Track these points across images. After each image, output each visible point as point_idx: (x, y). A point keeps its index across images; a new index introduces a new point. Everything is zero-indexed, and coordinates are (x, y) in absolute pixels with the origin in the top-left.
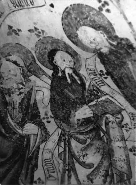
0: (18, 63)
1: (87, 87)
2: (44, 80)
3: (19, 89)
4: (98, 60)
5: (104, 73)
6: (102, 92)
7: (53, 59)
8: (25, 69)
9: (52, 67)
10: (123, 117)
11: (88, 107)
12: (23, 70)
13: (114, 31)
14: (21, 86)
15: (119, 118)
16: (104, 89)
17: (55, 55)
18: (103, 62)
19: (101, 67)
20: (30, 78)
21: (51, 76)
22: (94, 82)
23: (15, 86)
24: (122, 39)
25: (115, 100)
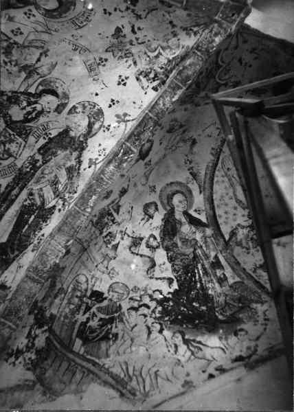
0: (39, 63)
1: (27, 124)
2: (23, 86)
3: (10, 62)
4: (61, 130)
5: (50, 136)
6: (27, 136)
7: (48, 93)
8: (32, 68)
9: (38, 92)
10: (7, 159)
11: (4, 127)
12: (30, 66)
13: (91, 137)
14: (13, 63)
15: (3, 155)
16: (32, 139)
17: (52, 95)
18: (60, 134)
19: (54, 133)
20: (23, 73)
21: (29, 91)
22: (36, 130)
23: (14, 58)
24: (86, 143)
25: (23, 150)
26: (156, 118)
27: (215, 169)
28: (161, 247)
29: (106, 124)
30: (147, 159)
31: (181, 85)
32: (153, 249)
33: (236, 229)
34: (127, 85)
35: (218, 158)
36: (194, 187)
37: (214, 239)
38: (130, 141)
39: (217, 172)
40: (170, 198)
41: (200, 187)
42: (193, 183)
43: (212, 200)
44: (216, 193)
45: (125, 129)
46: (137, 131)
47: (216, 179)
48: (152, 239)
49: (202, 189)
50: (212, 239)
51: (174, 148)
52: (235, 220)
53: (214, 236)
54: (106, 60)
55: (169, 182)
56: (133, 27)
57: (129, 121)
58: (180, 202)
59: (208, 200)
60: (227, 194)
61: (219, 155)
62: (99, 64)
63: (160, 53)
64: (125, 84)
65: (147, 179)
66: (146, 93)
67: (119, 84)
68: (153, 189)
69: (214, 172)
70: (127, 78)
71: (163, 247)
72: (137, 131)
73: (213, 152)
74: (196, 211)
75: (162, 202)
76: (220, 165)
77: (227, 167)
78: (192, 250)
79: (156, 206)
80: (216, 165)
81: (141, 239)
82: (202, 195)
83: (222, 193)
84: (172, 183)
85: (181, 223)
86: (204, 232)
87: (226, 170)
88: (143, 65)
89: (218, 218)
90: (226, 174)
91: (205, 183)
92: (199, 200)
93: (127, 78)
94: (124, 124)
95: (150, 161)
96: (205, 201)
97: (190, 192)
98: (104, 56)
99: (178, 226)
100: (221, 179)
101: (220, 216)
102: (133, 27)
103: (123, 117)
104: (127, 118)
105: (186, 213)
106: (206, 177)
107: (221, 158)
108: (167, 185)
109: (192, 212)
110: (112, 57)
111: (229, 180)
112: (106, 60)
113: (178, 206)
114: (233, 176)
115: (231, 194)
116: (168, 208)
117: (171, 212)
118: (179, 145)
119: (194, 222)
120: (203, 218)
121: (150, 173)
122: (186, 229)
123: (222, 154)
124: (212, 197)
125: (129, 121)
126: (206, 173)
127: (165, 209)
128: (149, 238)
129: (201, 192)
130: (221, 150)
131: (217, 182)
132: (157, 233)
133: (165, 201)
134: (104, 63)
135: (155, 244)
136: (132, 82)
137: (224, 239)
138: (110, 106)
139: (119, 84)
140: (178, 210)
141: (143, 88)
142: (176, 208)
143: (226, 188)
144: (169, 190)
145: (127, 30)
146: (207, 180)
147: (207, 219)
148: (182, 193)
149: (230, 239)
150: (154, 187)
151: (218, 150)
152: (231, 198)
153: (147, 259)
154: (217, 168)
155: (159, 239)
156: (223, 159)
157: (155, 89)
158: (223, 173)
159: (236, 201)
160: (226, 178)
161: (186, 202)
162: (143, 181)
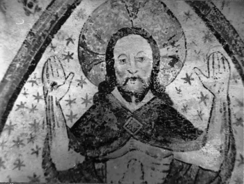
27: (26, 77)
39: (27, 85)
44: (11, 128)
47: (20, 99)
61: (42, 51)
69: (22, 83)
76: (38, 72)
77: (52, 79)
83: (22, 135)
87: (48, 86)
90: (46, 95)
111: (47, 109)
114: (57, 104)
115: (40, 143)
123: (48, 49)
130: (48, 42)
131: (22, 106)
143: (34, 125)
151: (43, 40)
154: (31, 77)
158: (41, 94)
159: (44, 163)
160: (42, 102)
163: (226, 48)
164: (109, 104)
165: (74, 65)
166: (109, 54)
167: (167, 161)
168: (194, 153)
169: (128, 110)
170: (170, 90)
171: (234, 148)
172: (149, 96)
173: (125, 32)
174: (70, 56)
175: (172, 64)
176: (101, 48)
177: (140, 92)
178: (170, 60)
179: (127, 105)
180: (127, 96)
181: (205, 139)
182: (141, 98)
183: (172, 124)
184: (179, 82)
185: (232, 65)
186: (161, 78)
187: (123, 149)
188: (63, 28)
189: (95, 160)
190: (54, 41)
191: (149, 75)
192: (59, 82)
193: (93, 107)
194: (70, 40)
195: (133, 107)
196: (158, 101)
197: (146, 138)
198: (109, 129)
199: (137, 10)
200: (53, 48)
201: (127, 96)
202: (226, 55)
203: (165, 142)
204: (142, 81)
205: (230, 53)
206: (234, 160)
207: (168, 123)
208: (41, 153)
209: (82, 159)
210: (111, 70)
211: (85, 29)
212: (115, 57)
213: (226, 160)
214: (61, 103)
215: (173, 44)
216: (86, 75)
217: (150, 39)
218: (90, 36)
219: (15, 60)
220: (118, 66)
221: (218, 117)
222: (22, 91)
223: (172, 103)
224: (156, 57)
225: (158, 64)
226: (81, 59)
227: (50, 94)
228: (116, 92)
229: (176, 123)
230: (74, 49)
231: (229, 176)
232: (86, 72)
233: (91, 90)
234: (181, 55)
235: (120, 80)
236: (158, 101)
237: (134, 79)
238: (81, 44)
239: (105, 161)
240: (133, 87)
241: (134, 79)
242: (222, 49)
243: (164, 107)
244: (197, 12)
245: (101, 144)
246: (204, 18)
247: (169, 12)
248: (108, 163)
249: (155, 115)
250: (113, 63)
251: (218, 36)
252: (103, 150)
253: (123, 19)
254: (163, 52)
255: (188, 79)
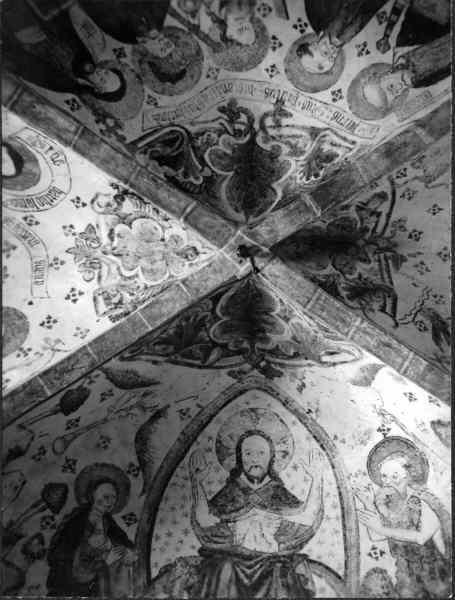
26: (95, 357)
27: (178, 464)
28: (45, 559)
29: (26, 346)
30: (73, 416)
31: (147, 323)
32: (31, 557)
33: (175, 564)
34: (78, 302)
35: (186, 451)
36: (137, 485)
37: (134, 571)
38: (45, 377)
39: (178, 469)
40: (93, 485)
41: (145, 484)
42: (136, 476)
43: (157, 509)
44: (167, 499)
45: (49, 361)
46: (62, 366)
48: (36, 541)
49: (147, 489)
50: (131, 569)
51: (124, 413)
52: (178, 550)
53: (136, 564)
54: (62, 263)
55: (100, 462)
56: (112, 231)
57: (59, 350)
58: (106, 497)
59: (150, 508)
60: (182, 507)
62: (51, 265)
63: (137, 276)
64: (75, 301)
65: (66, 447)
66: (98, 321)
67: (68, 298)
68: (70, 465)
69: (175, 469)
70: (81, 293)
71: (48, 559)
72: (62, 366)
73: (182, 437)
74: (124, 517)
75: (77, 489)
76: (186, 460)
78: (91, 577)
79: (66, 491)
80: (182, 458)
81: (20, 537)
82: (144, 497)
84: (104, 465)
85: (93, 530)
86: (123, 554)
87: (194, 470)
88: (110, 282)
89: (153, 540)
91: (155, 479)
92: (136, 503)
93: (81, 293)
94: (51, 352)
95: (77, 420)
96: (144, 507)
97: (128, 487)
98: (63, 256)
99: (87, 533)
100: (180, 481)
101: (158, 538)
102: (112, 231)
103: (53, 344)
104: (58, 347)
105: (107, 517)
106: (159, 471)
107: (191, 451)
108: (96, 465)
109: (117, 518)
110: (72, 261)
112: (62, 263)
113: (100, 502)
114: (201, 485)
115: (188, 508)
116: (84, 501)
117: (84, 510)
118: (132, 411)
119: (115, 535)
120: (131, 537)
121: (75, 437)
122: (97, 540)
123: (195, 444)
124: (158, 504)
125: (59, 350)
126: (162, 467)
127: (78, 499)
128: (33, 538)
129: (144, 491)
130: (195, 439)
131: (174, 484)
132: (48, 535)
133: (83, 489)
134: (59, 265)
135: (35, 548)
136: (85, 302)
137: (149, 573)
138: (42, 324)
139: (68, 298)
140: (97, 509)
141: (97, 312)
142: (95, 505)
144: (97, 473)
145: (103, 233)
146: (159, 479)
147: (136, 535)
148: (114, 484)
149: (158, 577)
150: (75, 462)
152: (186, 516)
153: (15, 572)
154: (181, 465)
155: (47, 545)
156: (193, 453)
157: (113, 319)
159: (192, 522)
161: (114, 500)
162: (59, 446)
163: (322, 446)
164: (238, 485)
165: (212, 457)
166: (239, 449)
167: (278, 521)
168: (298, 516)
169: (251, 489)
170: (282, 475)
171: (323, 511)
172: (267, 479)
173: (250, 433)
174: (210, 450)
175: (284, 457)
176: (233, 445)
177: (260, 476)
178: (283, 454)
179: (251, 485)
180: (251, 479)
181: (305, 508)
182: (261, 480)
183: (283, 499)
184: (289, 469)
185: (326, 457)
186: (275, 467)
187: (248, 515)
188: (207, 429)
189: (228, 521)
190: (199, 439)
191: (267, 464)
192: (202, 468)
193: (226, 487)
194: (210, 438)
195: (255, 486)
196: (274, 483)
197: (264, 507)
198: (238, 502)
199: (259, 419)
200: (198, 443)
201: (251, 479)
202: (321, 450)
203: (277, 509)
204: (261, 468)
205: (324, 449)
206: (322, 518)
207: (280, 499)
208: (189, 516)
209: (218, 521)
210: (239, 460)
211: (221, 430)
212: (243, 450)
213: (317, 519)
214: (204, 483)
215: (284, 442)
216: (222, 464)
217: (268, 439)
218: (225, 436)
219: (171, 451)
220: (245, 458)
221: (315, 492)
222: (175, 474)
223: (283, 484)
224: (273, 452)
225: (274, 456)
226: (218, 452)
227: (195, 476)
228: (243, 476)
229: (286, 497)
230: (212, 444)
231: (317, 528)
232: (221, 461)
233: (225, 474)
234: (290, 451)
235: (246, 468)
236: (274, 483)
237: (256, 467)
238: (219, 441)
239: (235, 522)
240: (256, 472)
241: (256, 467)
242: (319, 448)
243: (278, 487)
244: (301, 421)
245: (233, 511)
246: (305, 424)
247: (282, 421)
248: (238, 523)
249: (272, 492)
250: (241, 455)
251: (315, 437)
252: (234, 514)
253: (250, 426)
254: (277, 448)
255: (295, 468)
